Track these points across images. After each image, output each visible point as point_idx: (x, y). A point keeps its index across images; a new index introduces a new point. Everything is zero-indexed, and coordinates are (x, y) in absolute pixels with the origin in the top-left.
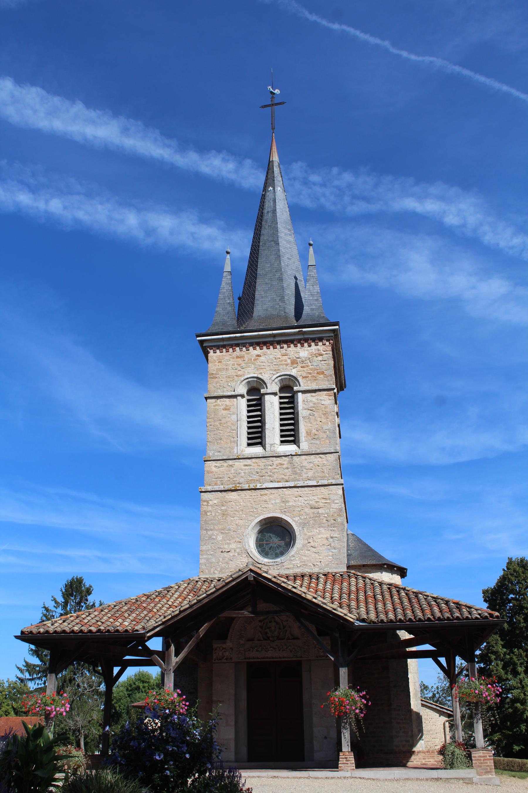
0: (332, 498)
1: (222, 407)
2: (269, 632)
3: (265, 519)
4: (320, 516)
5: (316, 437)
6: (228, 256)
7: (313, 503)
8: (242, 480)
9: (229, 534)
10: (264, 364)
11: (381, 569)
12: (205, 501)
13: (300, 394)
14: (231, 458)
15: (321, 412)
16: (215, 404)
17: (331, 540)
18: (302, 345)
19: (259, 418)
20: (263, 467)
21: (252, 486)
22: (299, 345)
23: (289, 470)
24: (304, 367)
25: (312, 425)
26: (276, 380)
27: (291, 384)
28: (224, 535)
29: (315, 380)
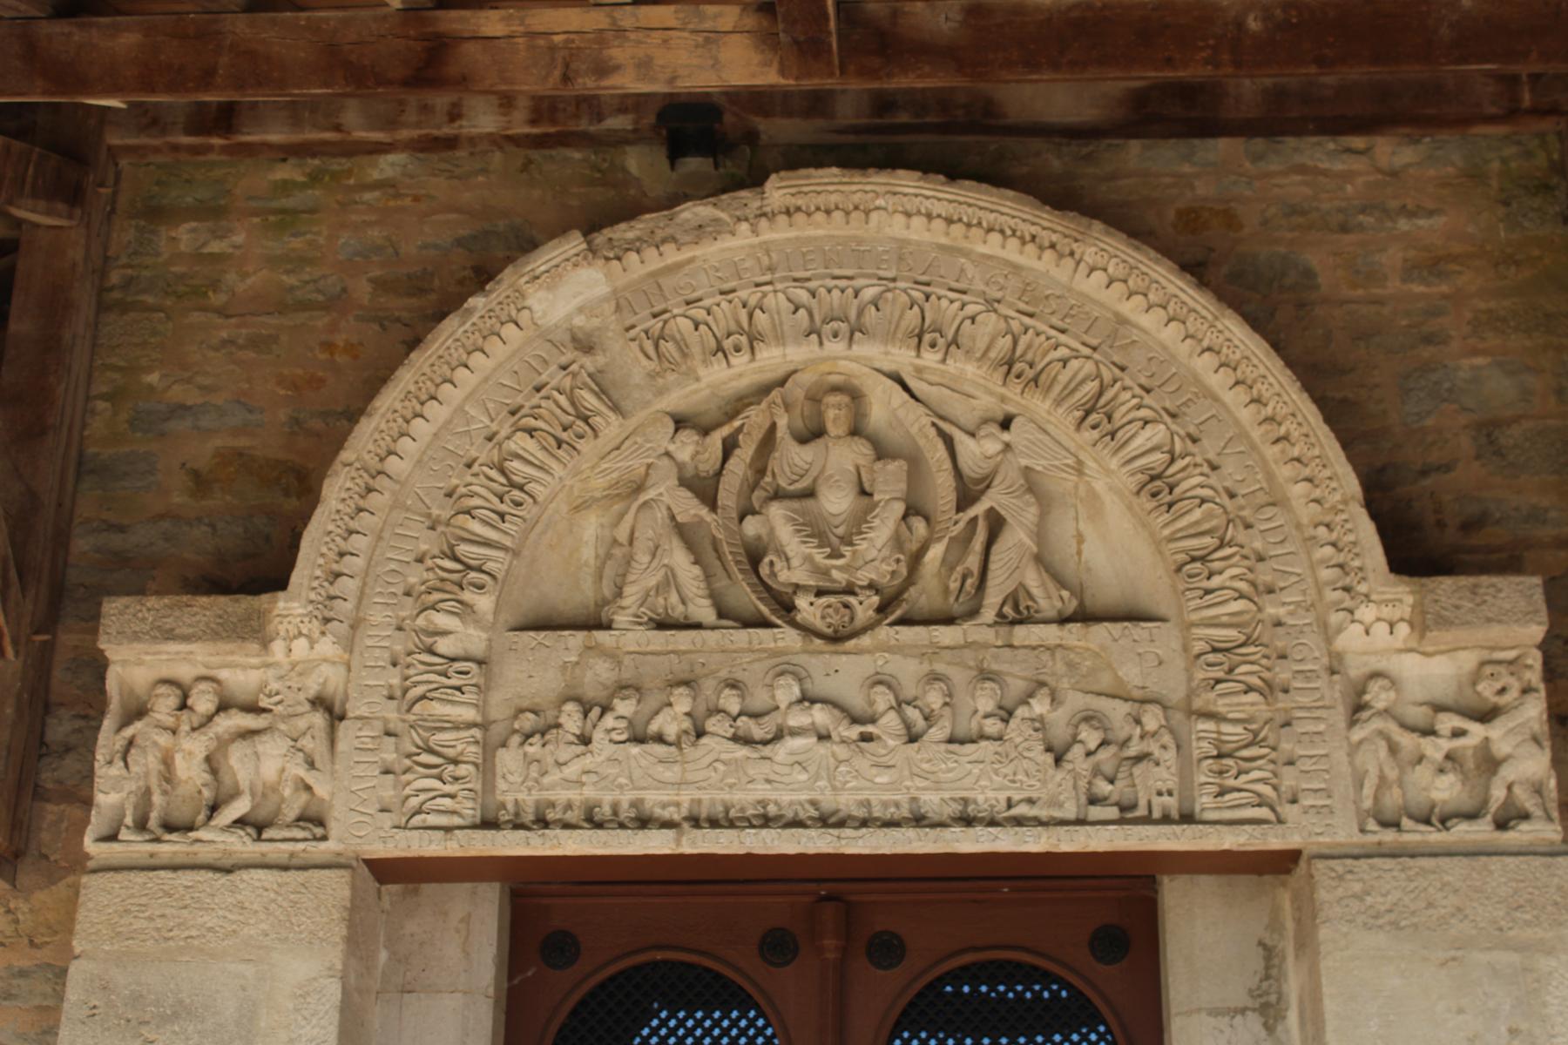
2: (786, 534)
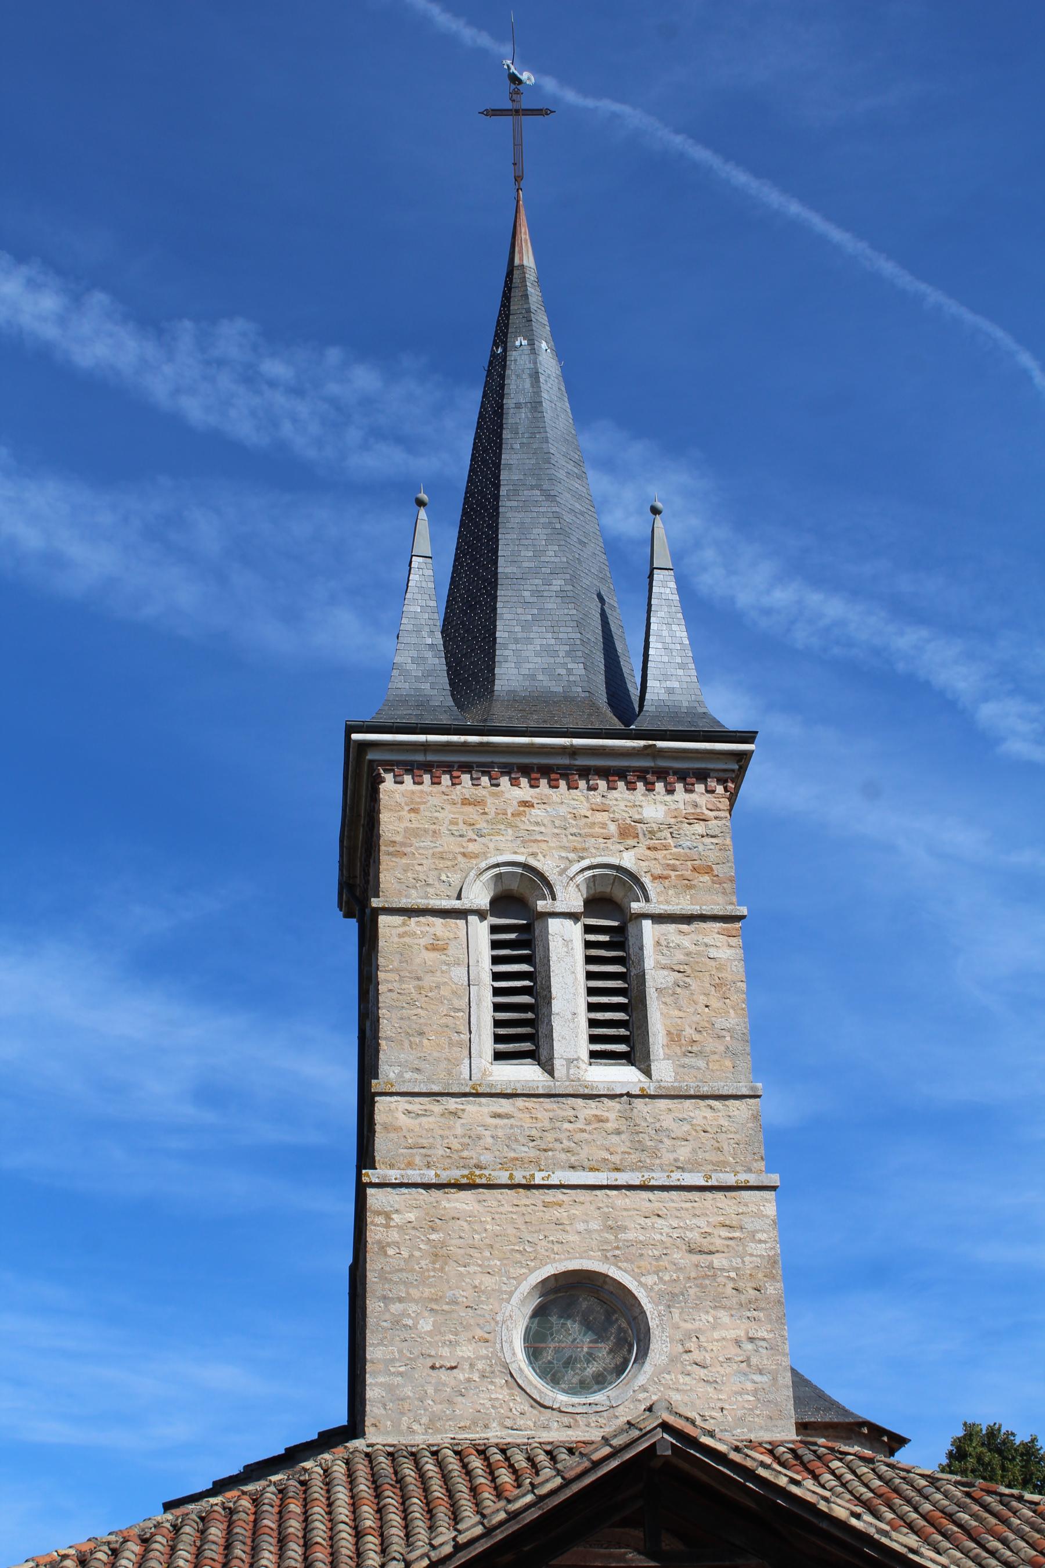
0: (750, 1227)
1: (423, 942)
3: (556, 1277)
4: (715, 1276)
5: (695, 1049)
6: (423, 514)
7: (693, 1235)
8: (486, 1158)
9: (455, 1315)
10: (543, 829)
12: (378, 1213)
13: (647, 924)
14: (455, 1089)
15: (707, 978)
16: (401, 930)
17: (749, 1347)
18: (650, 788)
19: (527, 983)
20: (547, 1125)
21: (519, 1179)
22: (640, 785)
23: (623, 1136)
24: (656, 849)
25: (681, 1014)
26: (580, 878)
27: (618, 894)
28: (440, 1318)
29: (690, 887)
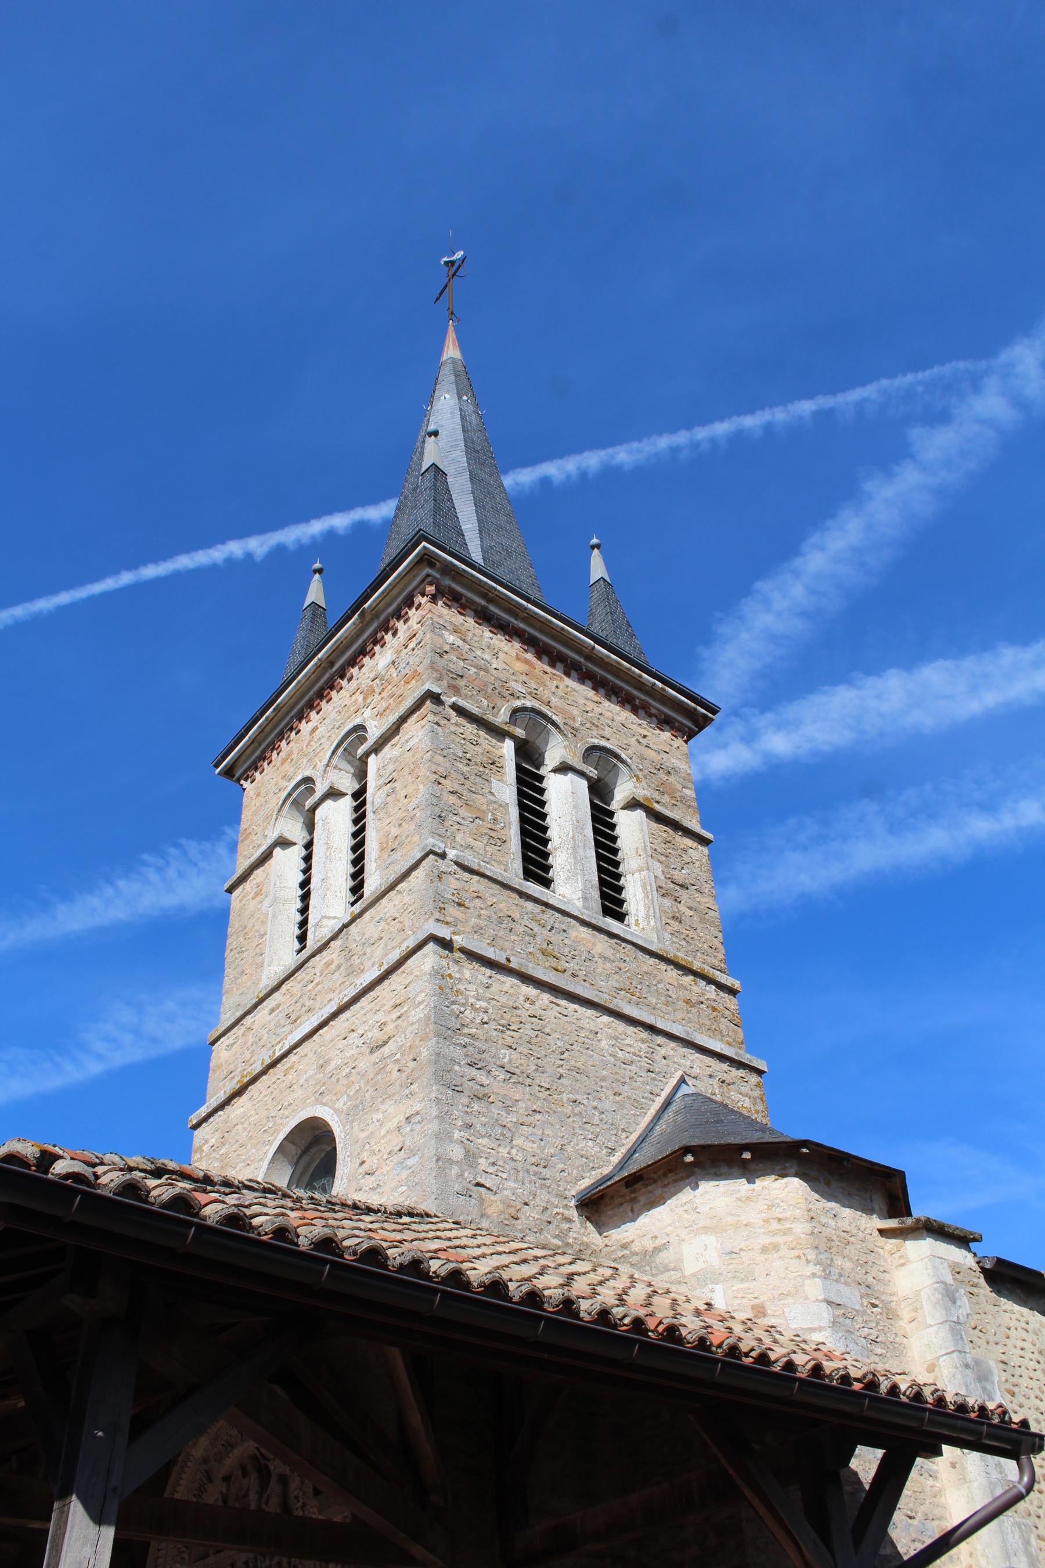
11: (688, 1177)
